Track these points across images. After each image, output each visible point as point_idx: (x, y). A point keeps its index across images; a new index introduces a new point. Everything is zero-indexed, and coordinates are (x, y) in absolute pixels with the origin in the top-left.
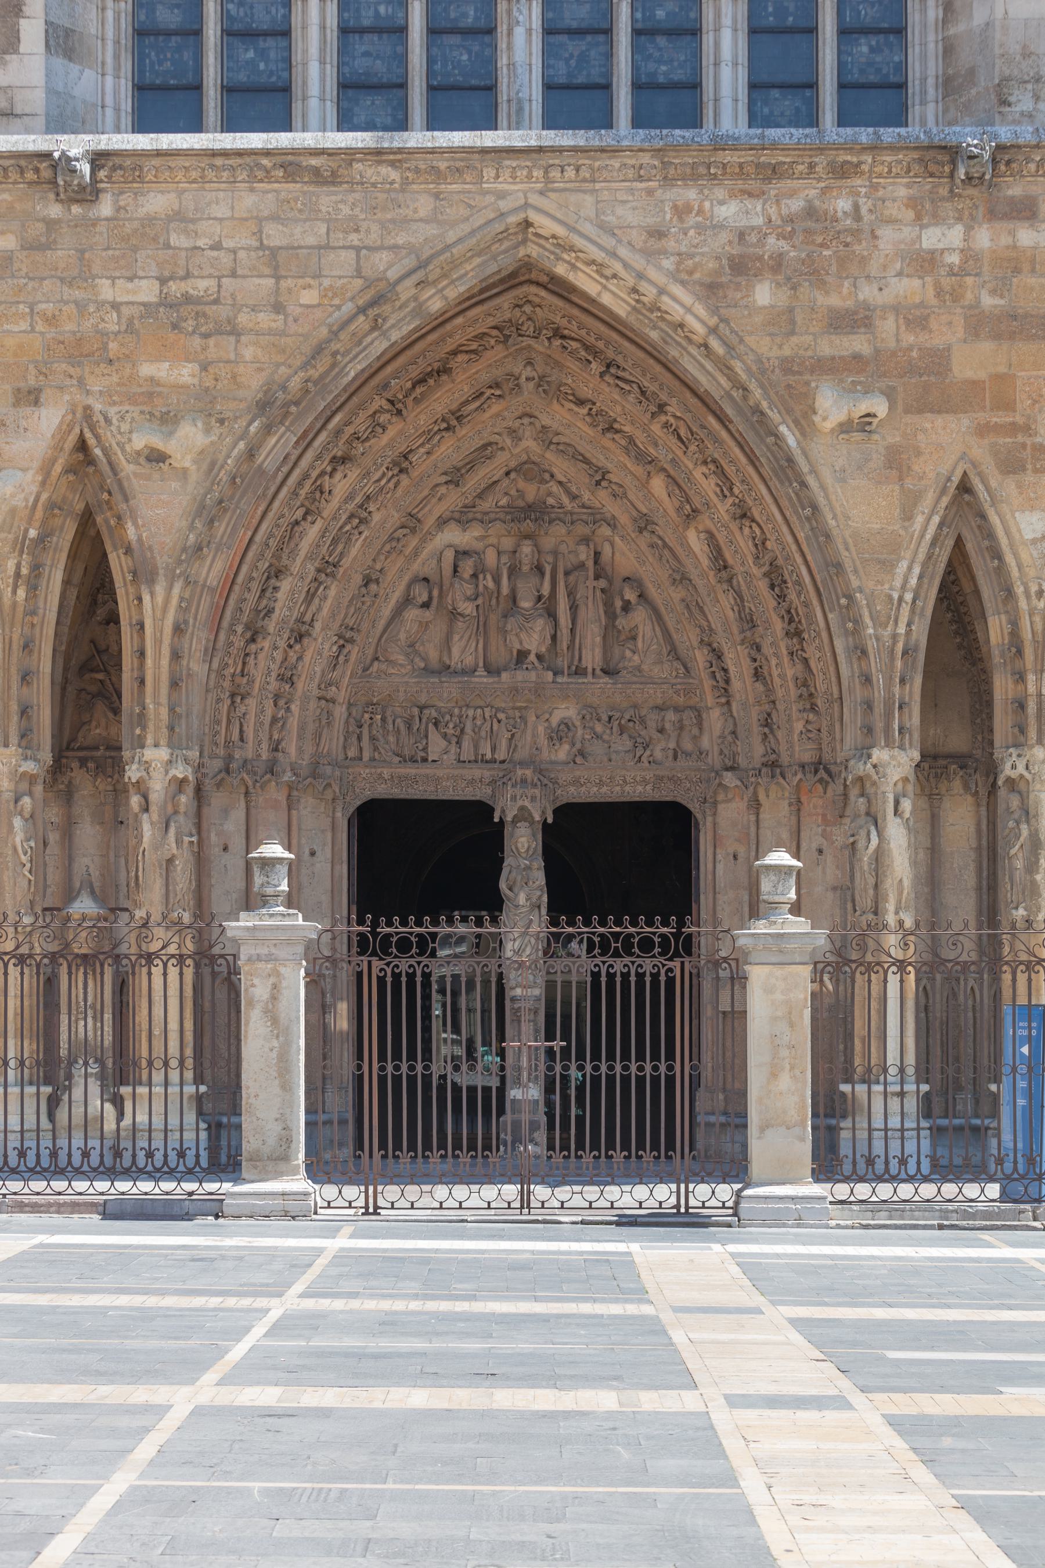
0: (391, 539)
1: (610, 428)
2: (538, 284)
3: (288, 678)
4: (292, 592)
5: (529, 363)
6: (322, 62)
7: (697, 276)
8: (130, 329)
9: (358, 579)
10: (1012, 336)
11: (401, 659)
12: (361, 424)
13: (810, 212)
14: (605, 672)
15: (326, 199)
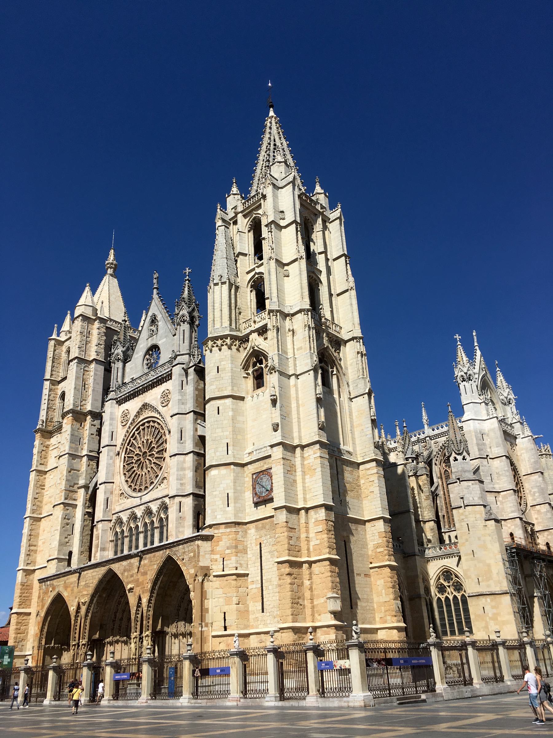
15: (97, 569)
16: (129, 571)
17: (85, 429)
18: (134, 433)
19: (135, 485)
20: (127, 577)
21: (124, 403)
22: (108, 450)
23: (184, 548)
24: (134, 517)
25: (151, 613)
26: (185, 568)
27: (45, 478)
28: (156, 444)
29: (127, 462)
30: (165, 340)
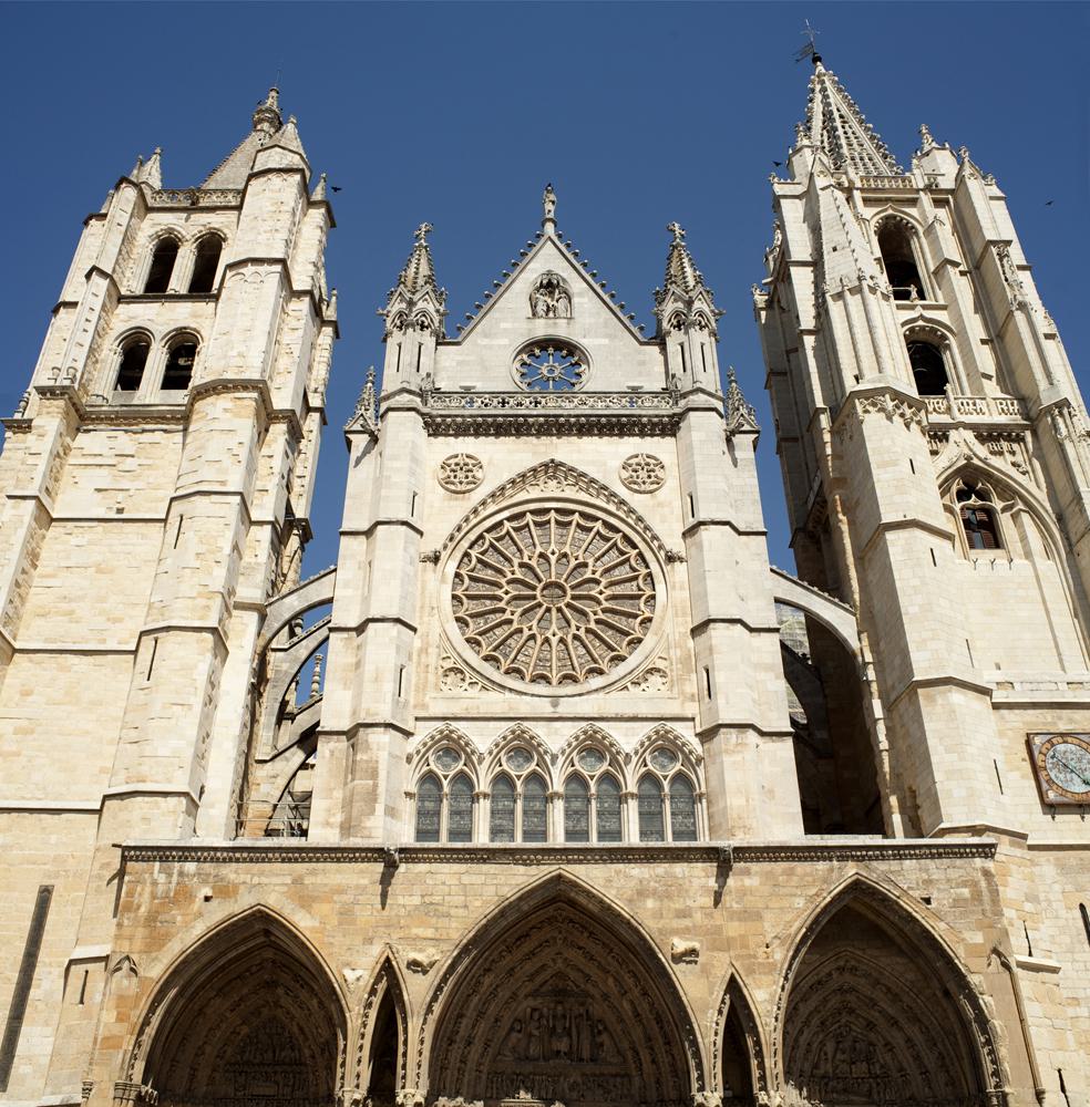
0: (506, 1003)
1: (591, 959)
2: (564, 902)
3: (463, 1062)
4: (467, 1026)
5: (560, 932)
6: (484, 821)
7: (625, 896)
8: (409, 915)
9: (493, 1020)
10: (745, 920)
11: (509, 1054)
12: (495, 955)
13: (666, 873)
14: (592, 1060)
15: (485, 867)
16: (669, 897)
17: (265, 451)
18: (500, 524)
19: (513, 662)
20: (658, 915)
21: (456, 435)
22: (406, 536)
23: (927, 871)
24: (523, 748)
25: (779, 1036)
26: (942, 925)
27: (44, 537)
28: (601, 576)
29: (466, 590)
30: (606, 341)
